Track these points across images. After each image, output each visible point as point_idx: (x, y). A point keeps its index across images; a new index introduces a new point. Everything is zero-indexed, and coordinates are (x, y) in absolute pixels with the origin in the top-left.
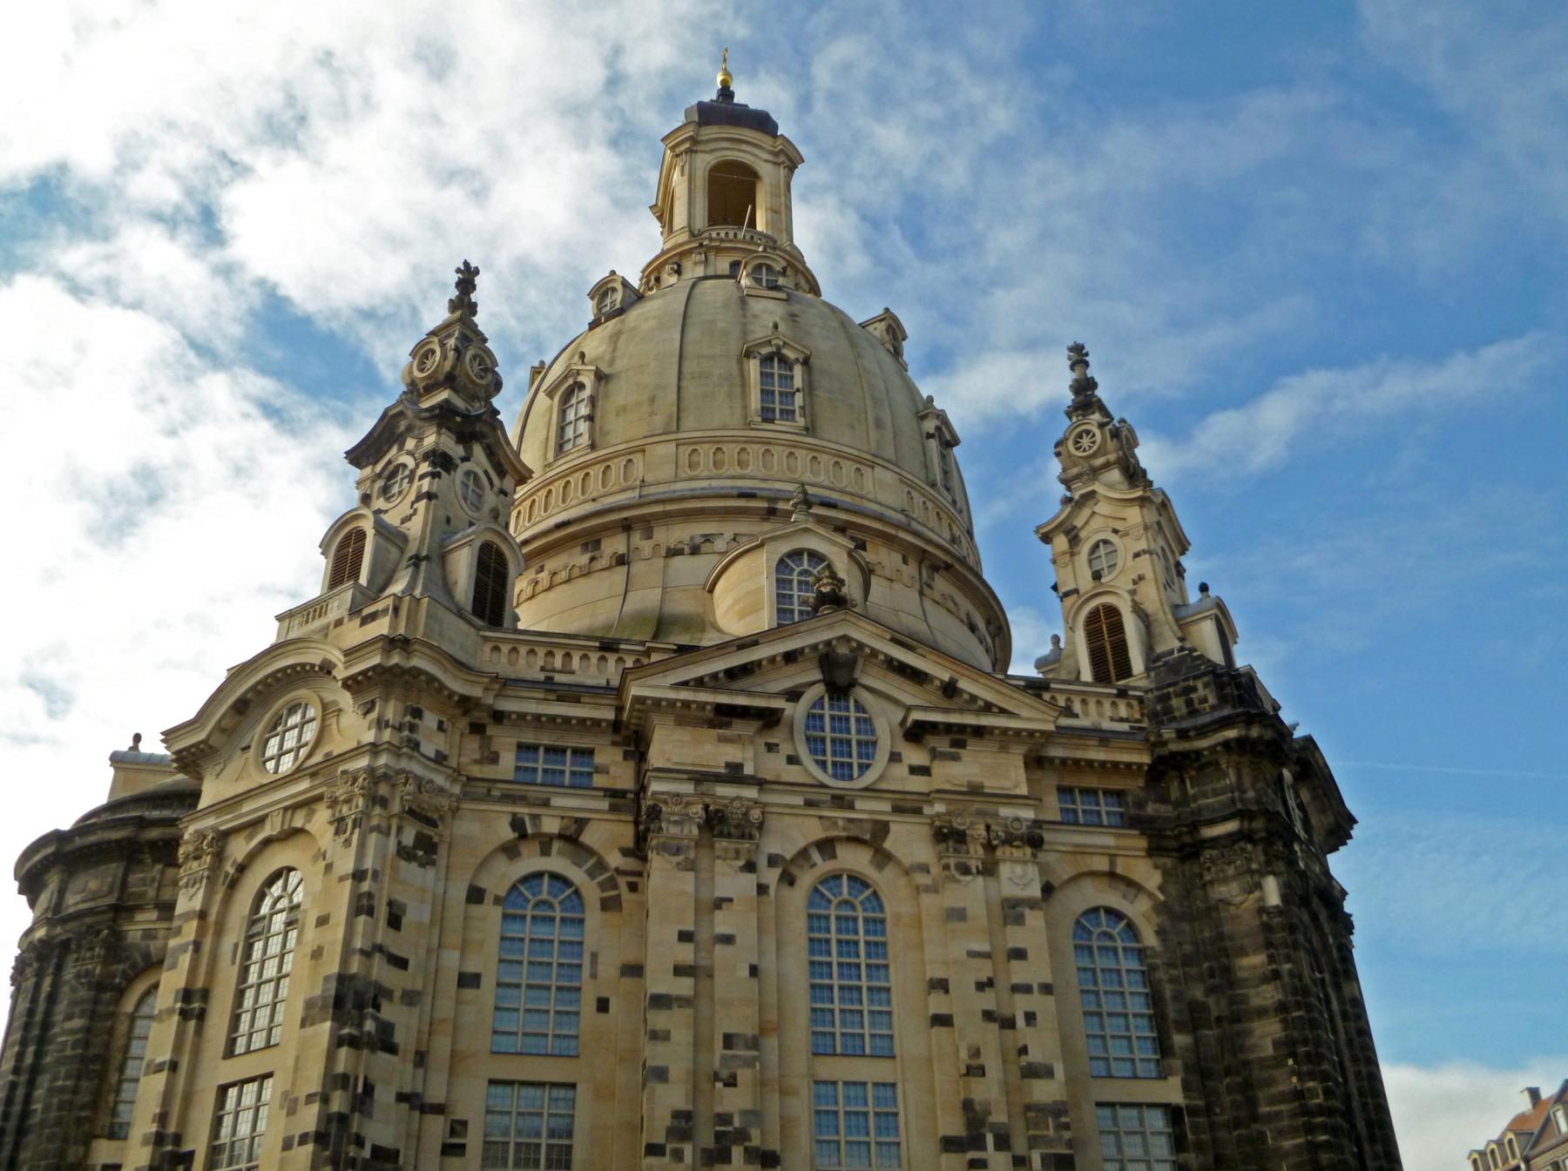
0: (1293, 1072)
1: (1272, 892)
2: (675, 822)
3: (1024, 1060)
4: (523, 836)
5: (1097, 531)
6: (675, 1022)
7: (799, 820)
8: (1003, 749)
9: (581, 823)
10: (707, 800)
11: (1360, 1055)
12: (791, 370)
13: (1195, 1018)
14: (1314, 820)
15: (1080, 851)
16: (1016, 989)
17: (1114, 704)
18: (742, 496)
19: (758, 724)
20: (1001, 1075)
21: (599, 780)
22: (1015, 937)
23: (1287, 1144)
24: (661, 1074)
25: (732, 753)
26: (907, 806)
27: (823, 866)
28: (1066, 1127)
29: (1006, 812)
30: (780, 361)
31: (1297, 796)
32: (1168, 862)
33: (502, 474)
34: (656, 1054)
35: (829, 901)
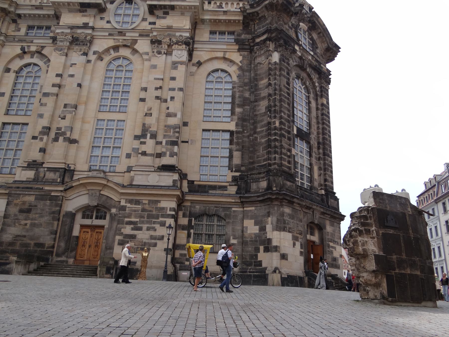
0: (269, 117)
1: (276, 57)
2: (61, 41)
4: (25, 53)
7: (106, 40)
8: (182, 14)
9: (43, 47)
10: (73, 34)
11: (321, 122)
13: (245, 102)
14: (319, 45)
15: (213, 50)
16: (170, 89)
17: (238, 4)
22: (174, 73)
23: (263, 140)
24: (41, 116)
25: (85, 20)
26: (144, 34)
28: (178, 132)
29: (178, 34)
31: (310, 34)
32: (246, 53)
34: (42, 110)
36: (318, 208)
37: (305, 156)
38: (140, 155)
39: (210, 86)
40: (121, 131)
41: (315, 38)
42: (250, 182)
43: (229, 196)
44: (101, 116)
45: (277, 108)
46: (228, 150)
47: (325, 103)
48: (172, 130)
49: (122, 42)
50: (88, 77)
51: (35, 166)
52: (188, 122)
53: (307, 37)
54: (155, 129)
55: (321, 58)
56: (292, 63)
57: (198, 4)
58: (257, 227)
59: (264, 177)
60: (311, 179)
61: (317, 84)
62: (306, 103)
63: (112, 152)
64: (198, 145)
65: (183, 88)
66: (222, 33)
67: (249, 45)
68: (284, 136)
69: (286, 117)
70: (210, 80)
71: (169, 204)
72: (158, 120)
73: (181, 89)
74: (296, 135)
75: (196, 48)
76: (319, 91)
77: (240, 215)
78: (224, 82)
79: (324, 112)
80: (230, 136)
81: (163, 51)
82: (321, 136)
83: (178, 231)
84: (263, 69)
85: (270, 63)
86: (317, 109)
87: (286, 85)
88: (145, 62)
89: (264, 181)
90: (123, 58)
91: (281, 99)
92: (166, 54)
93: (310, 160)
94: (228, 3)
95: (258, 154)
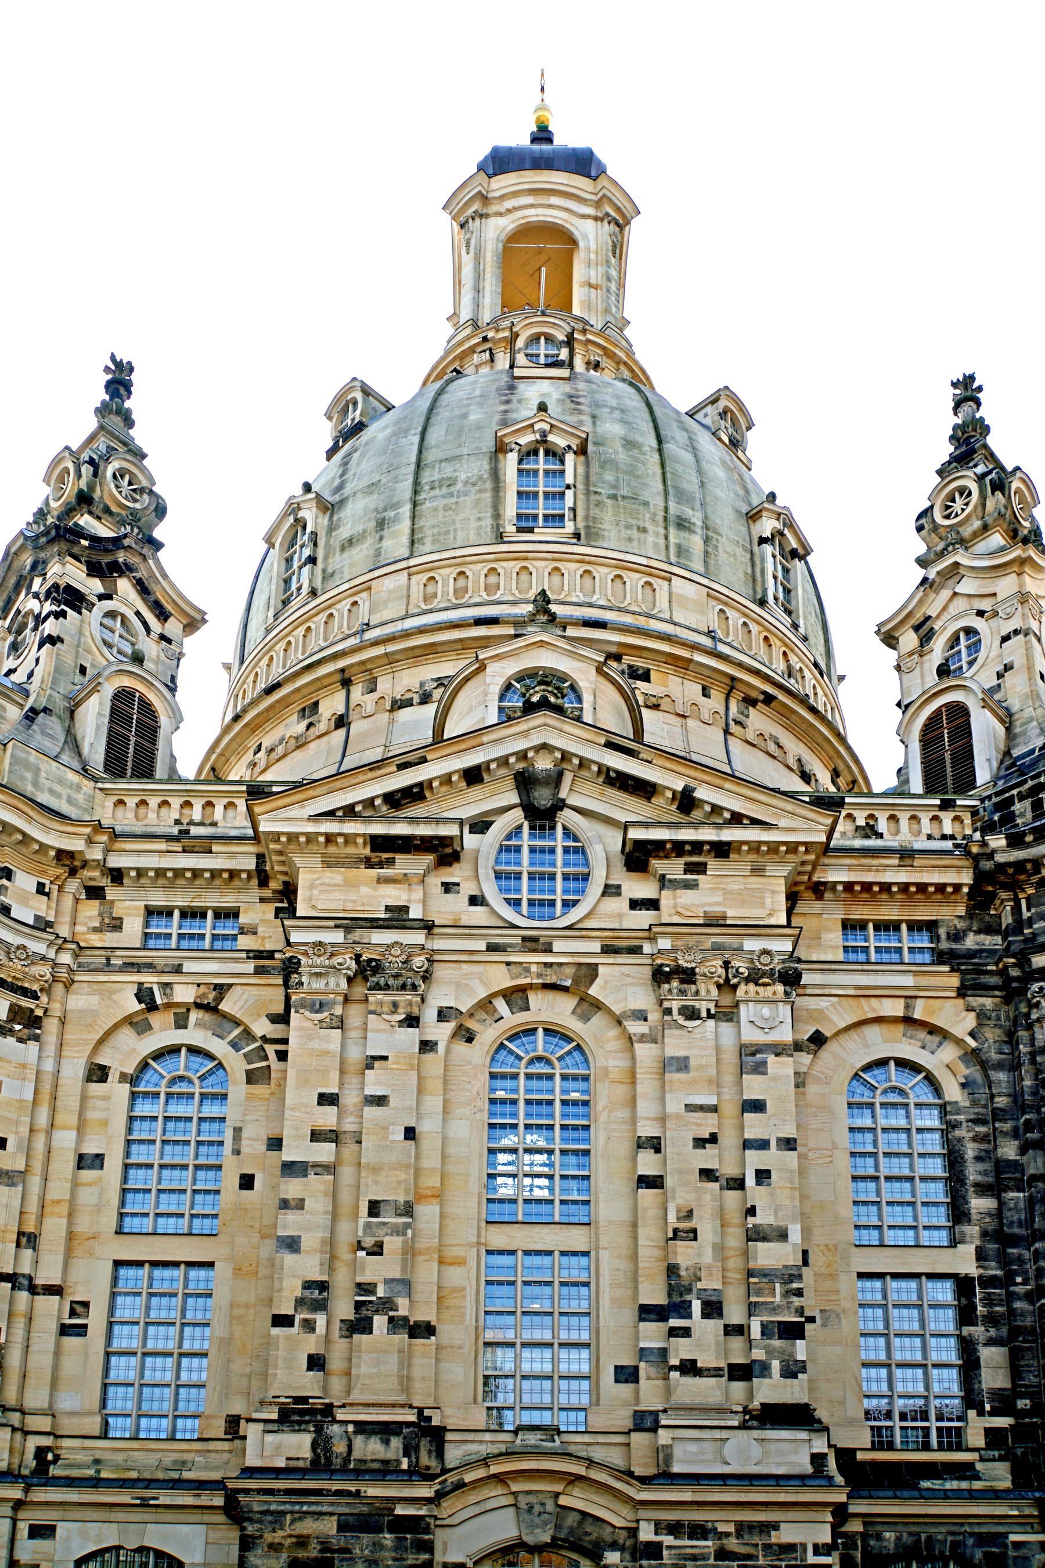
2: (318, 975)
6: (311, 1189)
7: (479, 968)
9: (221, 990)
10: (358, 948)
12: (562, 462)
16: (747, 1145)
18: (479, 622)
19: (429, 858)
20: (718, 1240)
21: (245, 942)
22: (754, 1087)
24: (292, 1244)
27: (511, 1020)
28: (799, 1293)
30: (547, 453)
32: (988, 1002)
33: (163, 615)
34: (290, 1224)
35: (519, 1058)
38: (675, 1375)
43: (994, 1495)
48: (777, 1286)
50: (433, 1103)
51: (307, 1418)
54: (717, 1285)
75: (805, 987)
81: (703, 1007)
88: (636, 1045)
90: (546, 1031)
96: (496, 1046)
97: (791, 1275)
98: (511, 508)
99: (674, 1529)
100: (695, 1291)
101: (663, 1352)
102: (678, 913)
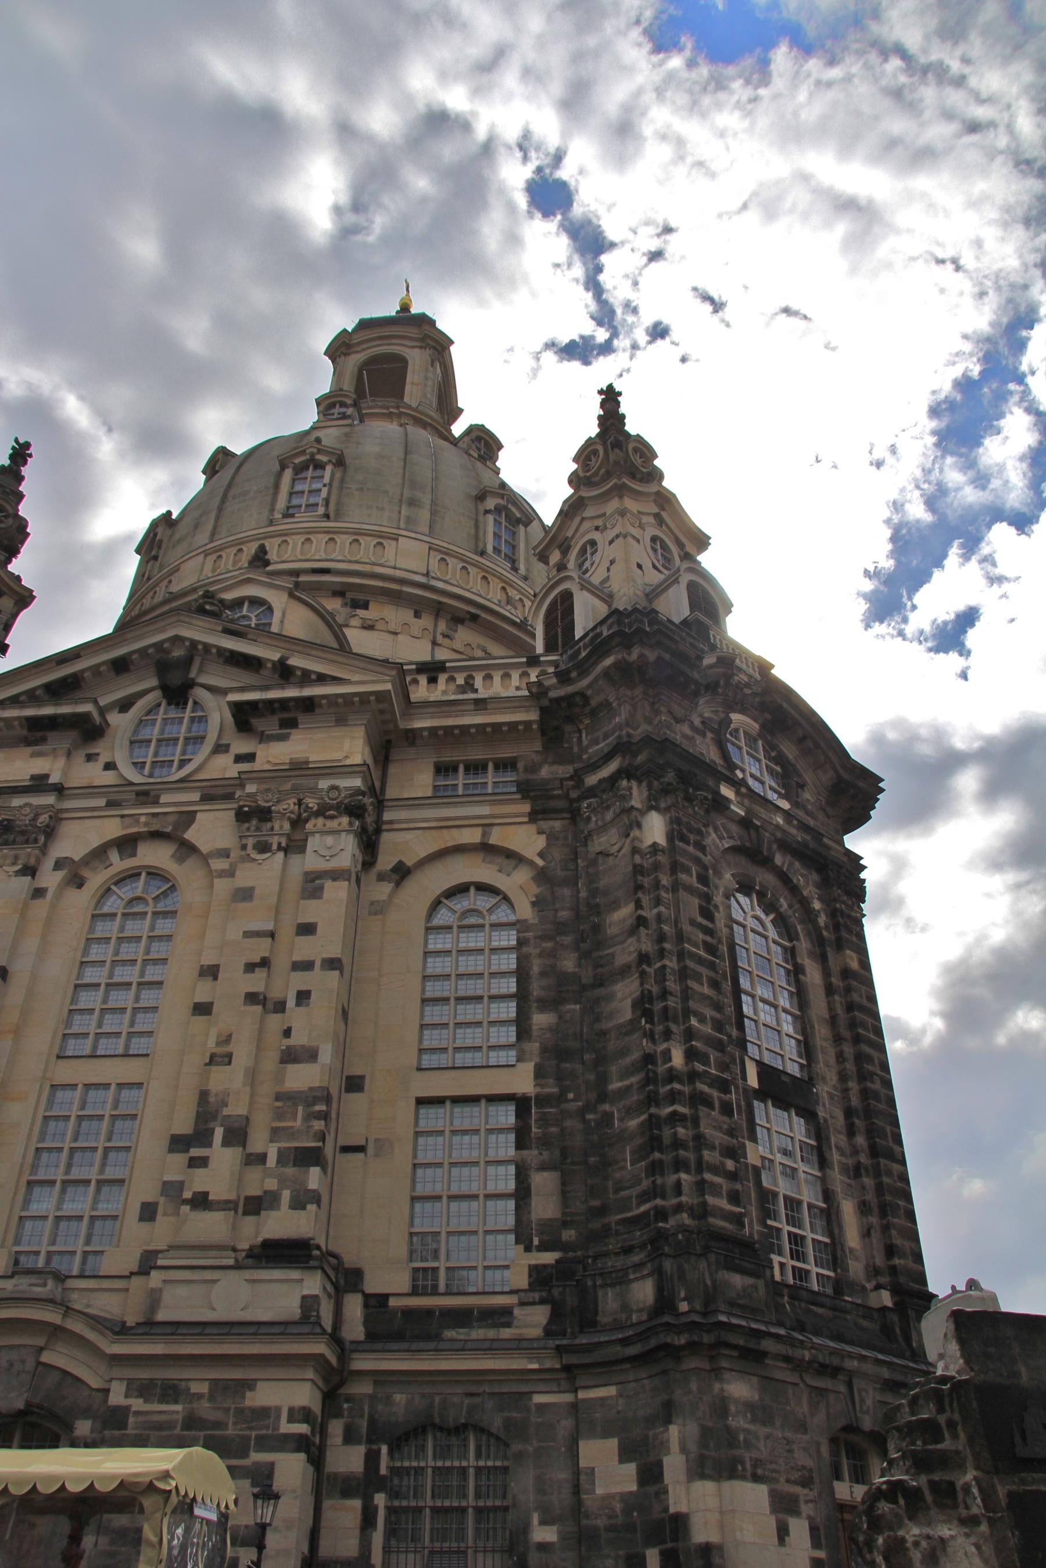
0: (645, 1035)
1: (655, 829)
3: (287, 1042)
5: (584, 535)
8: (341, 721)
11: (846, 1034)
13: (562, 990)
14: (808, 777)
17: (525, 674)
19: (73, 734)
22: (311, 911)
23: (633, 1123)
25: (39, 766)
26: (215, 794)
28: (325, 1116)
29: (324, 784)
31: (770, 747)
32: (557, 825)
36: (869, 1368)
37: (802, 1167)
38: (186, 1209)
39: (438, 942)
40: (128, 1123)
41: (790, 757)
42: (594, 1285)
43: (519, 1346)
44: (66, 1072)
45: (672, 1002)
46: (512, 1169)
47: (854, 965)
48: (300, 1108)
49: (146, 824)
50: (31, 944)
52: (362, 1078)
53: (762, 757)
54: (242, 1111)
55: (821, 816)
56: (717, 841)
57: (388, 686)
58: (631, 1468)
59: (640, 1265)
60: (833, 1253)
61: (817, 905)
62: (788, 972)
63: (96, 1201)
64: (402, 1156)
65: (339, 960)
66: (476, 768)
67: (567, 796)
68: (708, 1103)
69: (708, 1029)
70: (441, 923)
71: (289, 1394)
72: (252, 1076)
73: (333, 964)
74: (755, 1091)
75: (391, 822)
76: (826, 927)
77: (564, 1423)
78: (487, 927)
79: (855, 997)
80: (517, 1117)
81: (275, 841)
82: (853, 1085)
83: (327, 1504)
84: (615, 873)
85: (635, 851)
86: (830, 990)
87: (700, 920)
88: (217, 881)
89: (643, 1277)
90: (149, 874)
91: (685, 967)
92: (286, 850)
93: (823, 1180)
94: (493, 673)
95: (618, 1175)
96: (102, 890)
97: (314, 1097)
98: (281, 503)
99: (143, 1389)
100: (220, 1117)
101: (182, 1183)
102: (269, 762)
